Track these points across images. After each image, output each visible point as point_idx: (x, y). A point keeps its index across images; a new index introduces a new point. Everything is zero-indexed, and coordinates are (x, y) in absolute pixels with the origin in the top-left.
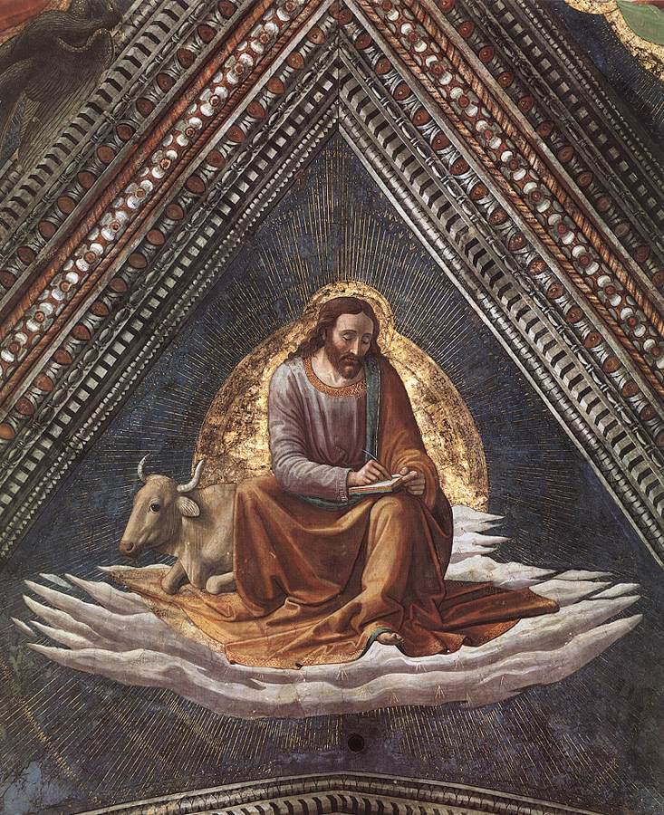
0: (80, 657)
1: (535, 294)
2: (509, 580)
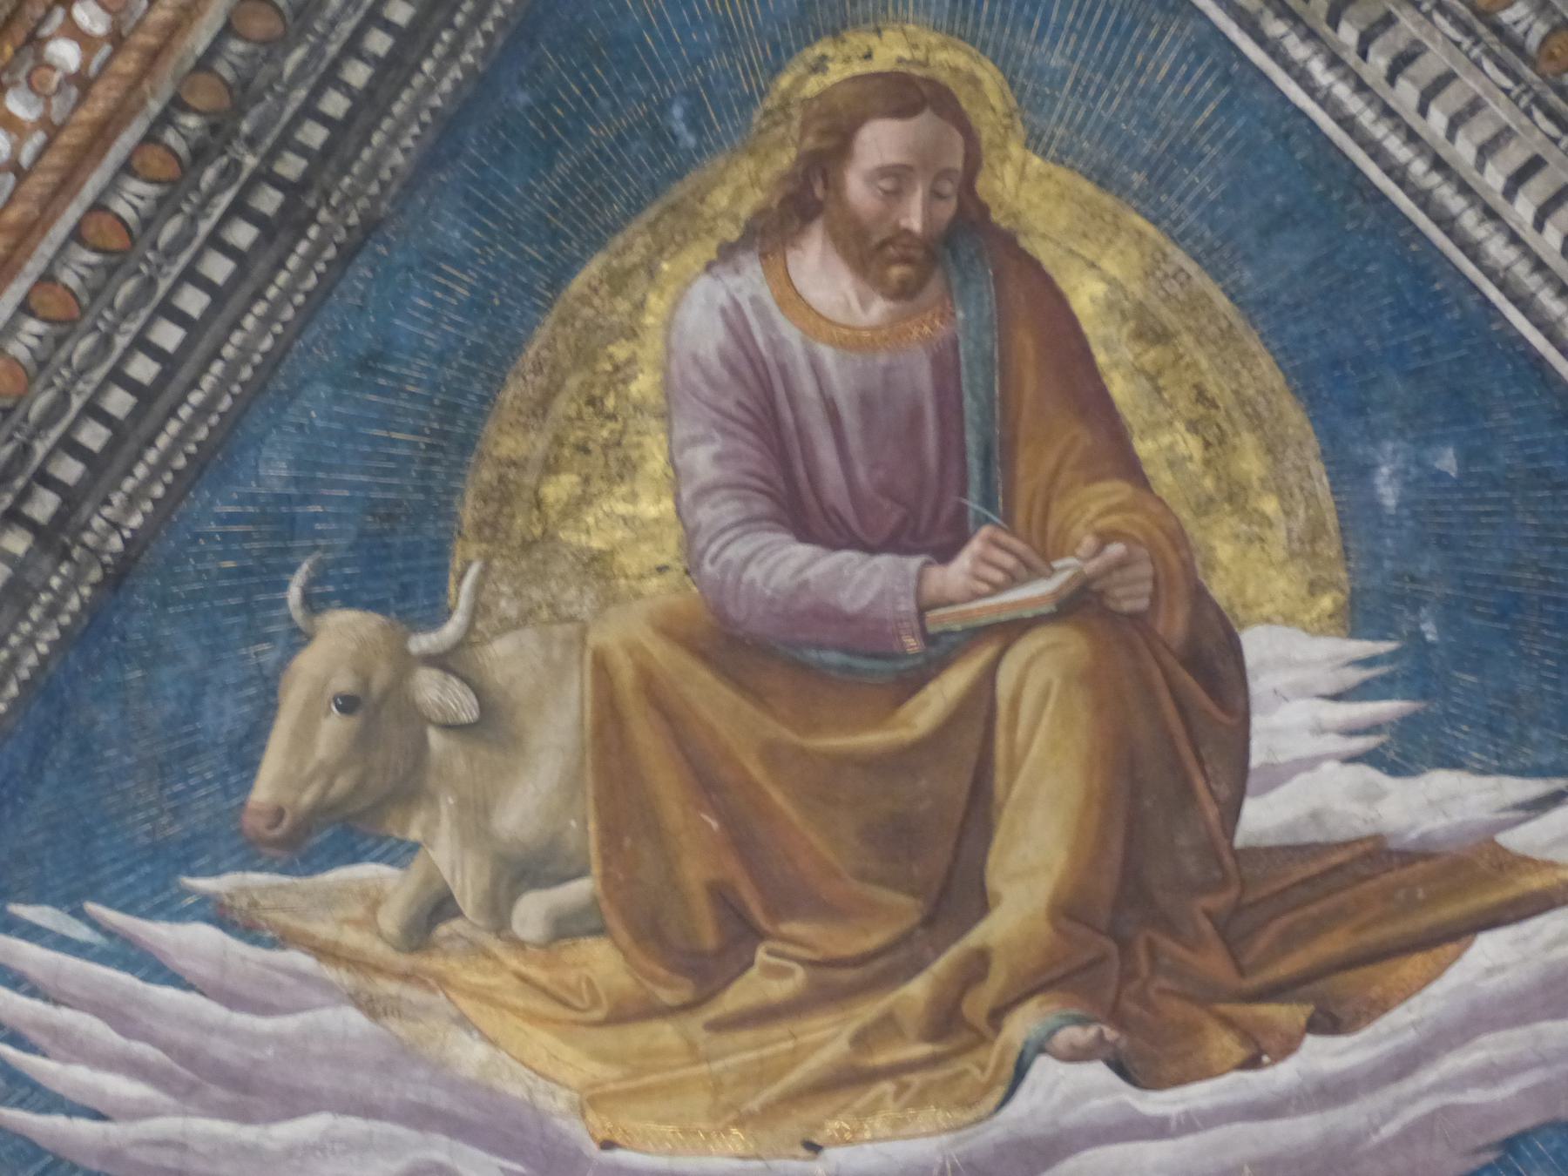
0: (139, 1143)
2: (1434, 824)
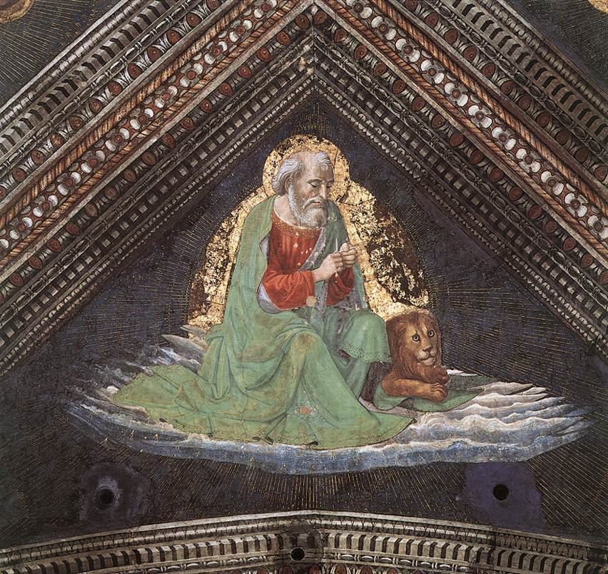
1: (34, 141)
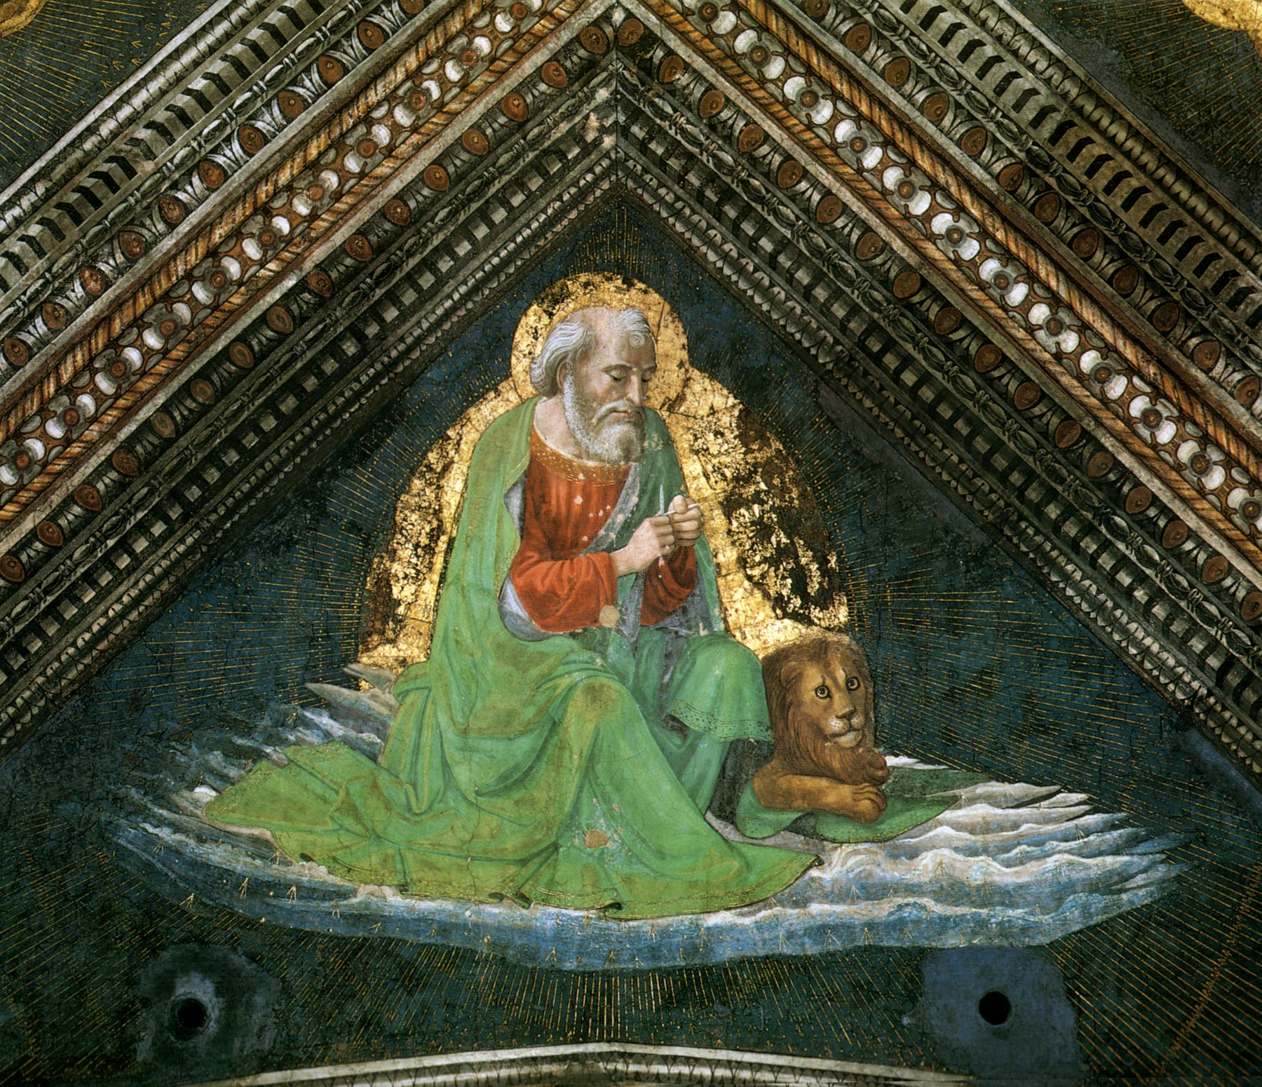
1: (44, 286)
